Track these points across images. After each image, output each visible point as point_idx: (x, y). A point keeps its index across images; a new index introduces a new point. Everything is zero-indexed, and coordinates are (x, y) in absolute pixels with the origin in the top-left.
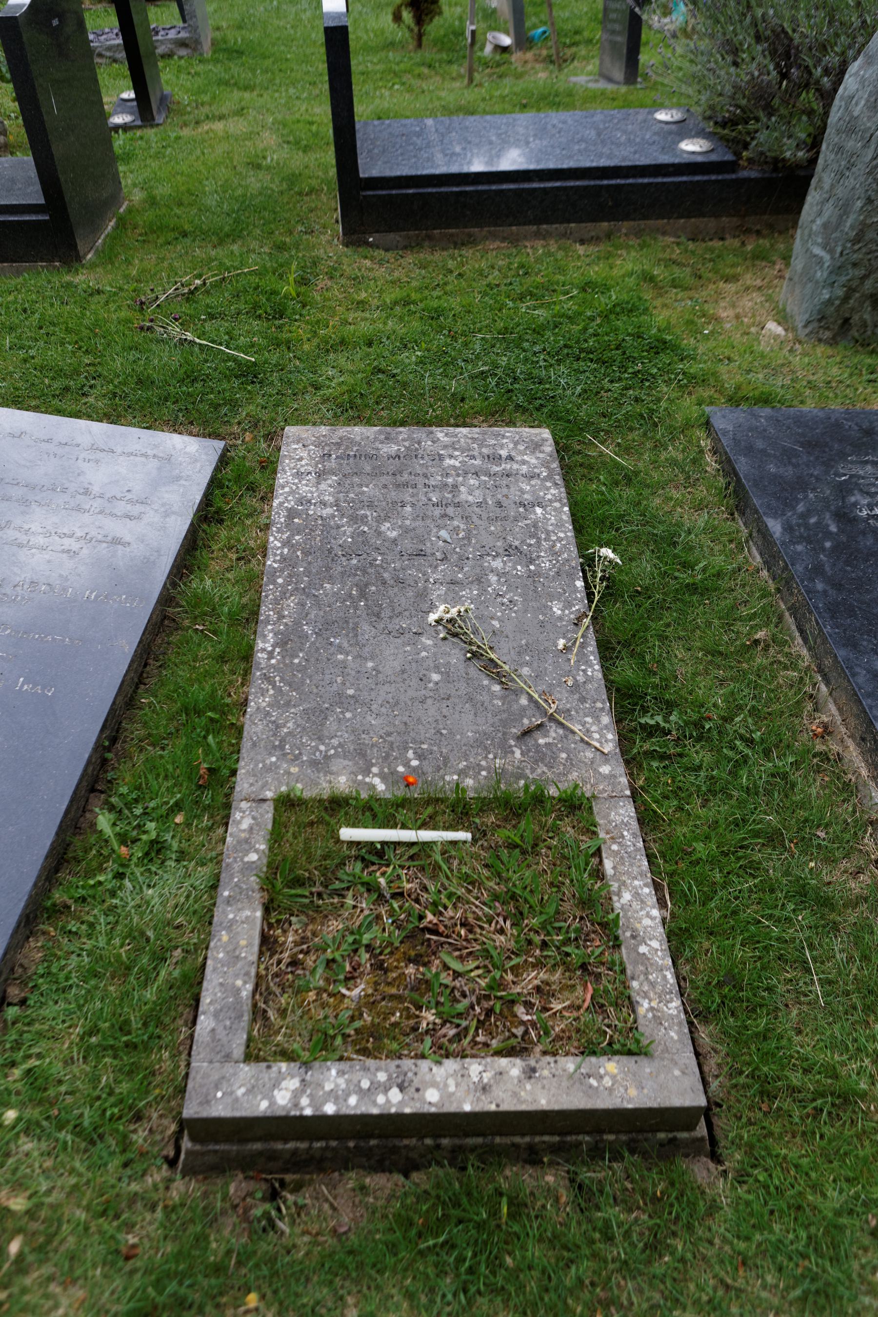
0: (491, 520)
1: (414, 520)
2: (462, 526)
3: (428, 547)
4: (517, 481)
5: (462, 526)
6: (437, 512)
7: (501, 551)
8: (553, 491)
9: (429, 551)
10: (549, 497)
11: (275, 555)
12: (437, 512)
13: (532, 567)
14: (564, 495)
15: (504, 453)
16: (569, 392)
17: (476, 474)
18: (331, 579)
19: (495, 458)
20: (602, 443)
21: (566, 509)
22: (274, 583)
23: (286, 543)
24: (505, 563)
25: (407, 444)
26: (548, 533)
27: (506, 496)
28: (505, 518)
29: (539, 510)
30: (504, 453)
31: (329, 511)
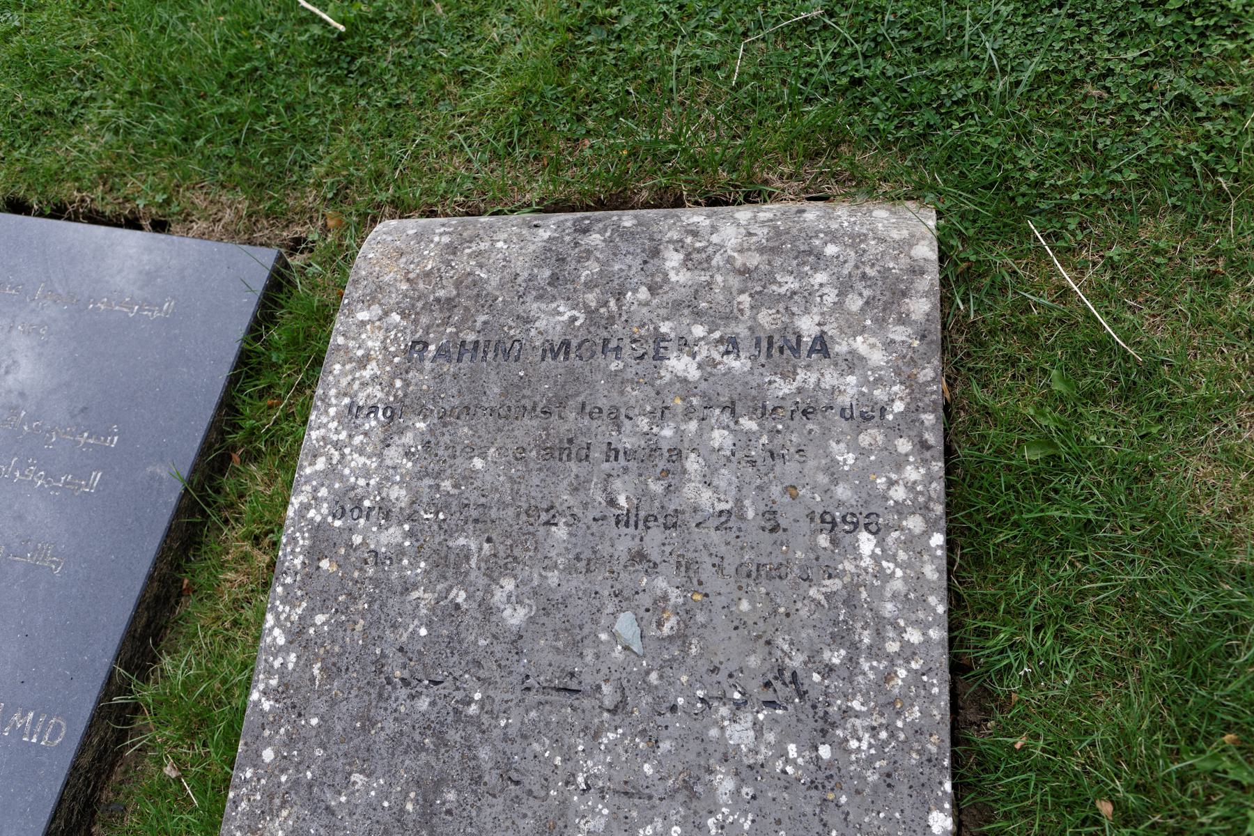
0: (751, 574)
1: (569, 570)
2: (675, 596)
3: (586, 666)
4: (826, 432)
5: (675, 596)
6: (624, 543)
7: (755, 687)
8: (912, 473)
9: (588, 680)
10: (899, 493)
11: (270, 672)
12: (624, 543)
13: (825, 752)
14: (938, 487)
15: (808, 326)
16: (999, 85)
17: (731, 407)
18: (365, 760)
19: (782, 348)
20: (1066, 253)
21: (938, 539)
22: (256, 761)
23: (297, 635)
24: (758, 728)
25: (591, 298)
26: (880, 625)
27: (791, 490)
28: (777, 573)
29: (866, 543)
30: (808, 326)
31: (393, 535)
